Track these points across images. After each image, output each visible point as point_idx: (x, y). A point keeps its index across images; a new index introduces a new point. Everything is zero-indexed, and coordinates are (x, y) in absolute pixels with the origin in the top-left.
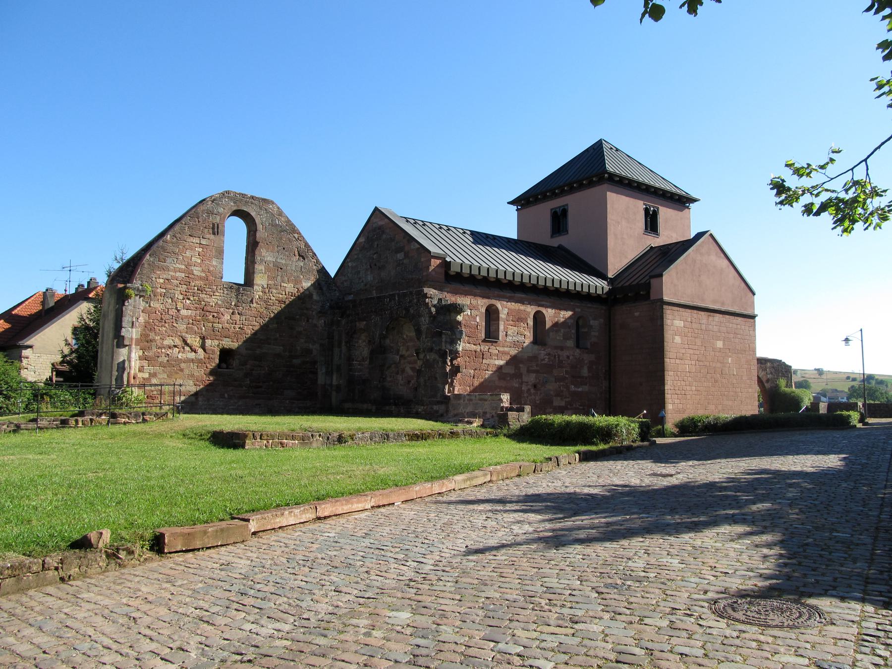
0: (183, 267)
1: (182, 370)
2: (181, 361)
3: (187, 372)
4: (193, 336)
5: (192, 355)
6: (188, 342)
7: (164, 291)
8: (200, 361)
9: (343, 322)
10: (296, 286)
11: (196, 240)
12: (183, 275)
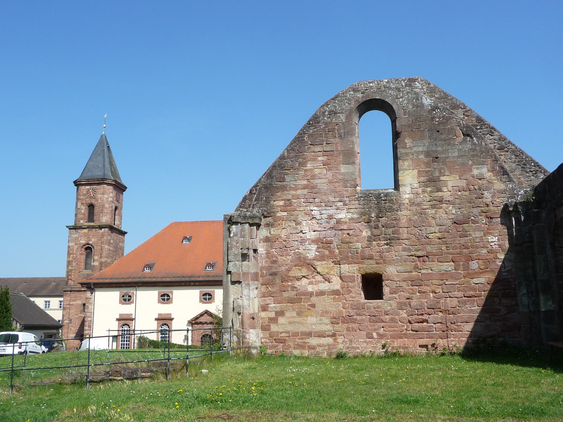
0: (305, 182)
1: (313, 306)
2: (311, 294)
3: (319, 308)
4: (324, 262)
5: (325, 286)
6: (319, 270)
7: (285, 214)
9: (544, 215)
10: (464, 177)
11: (318, 149)
12: (305, 191)
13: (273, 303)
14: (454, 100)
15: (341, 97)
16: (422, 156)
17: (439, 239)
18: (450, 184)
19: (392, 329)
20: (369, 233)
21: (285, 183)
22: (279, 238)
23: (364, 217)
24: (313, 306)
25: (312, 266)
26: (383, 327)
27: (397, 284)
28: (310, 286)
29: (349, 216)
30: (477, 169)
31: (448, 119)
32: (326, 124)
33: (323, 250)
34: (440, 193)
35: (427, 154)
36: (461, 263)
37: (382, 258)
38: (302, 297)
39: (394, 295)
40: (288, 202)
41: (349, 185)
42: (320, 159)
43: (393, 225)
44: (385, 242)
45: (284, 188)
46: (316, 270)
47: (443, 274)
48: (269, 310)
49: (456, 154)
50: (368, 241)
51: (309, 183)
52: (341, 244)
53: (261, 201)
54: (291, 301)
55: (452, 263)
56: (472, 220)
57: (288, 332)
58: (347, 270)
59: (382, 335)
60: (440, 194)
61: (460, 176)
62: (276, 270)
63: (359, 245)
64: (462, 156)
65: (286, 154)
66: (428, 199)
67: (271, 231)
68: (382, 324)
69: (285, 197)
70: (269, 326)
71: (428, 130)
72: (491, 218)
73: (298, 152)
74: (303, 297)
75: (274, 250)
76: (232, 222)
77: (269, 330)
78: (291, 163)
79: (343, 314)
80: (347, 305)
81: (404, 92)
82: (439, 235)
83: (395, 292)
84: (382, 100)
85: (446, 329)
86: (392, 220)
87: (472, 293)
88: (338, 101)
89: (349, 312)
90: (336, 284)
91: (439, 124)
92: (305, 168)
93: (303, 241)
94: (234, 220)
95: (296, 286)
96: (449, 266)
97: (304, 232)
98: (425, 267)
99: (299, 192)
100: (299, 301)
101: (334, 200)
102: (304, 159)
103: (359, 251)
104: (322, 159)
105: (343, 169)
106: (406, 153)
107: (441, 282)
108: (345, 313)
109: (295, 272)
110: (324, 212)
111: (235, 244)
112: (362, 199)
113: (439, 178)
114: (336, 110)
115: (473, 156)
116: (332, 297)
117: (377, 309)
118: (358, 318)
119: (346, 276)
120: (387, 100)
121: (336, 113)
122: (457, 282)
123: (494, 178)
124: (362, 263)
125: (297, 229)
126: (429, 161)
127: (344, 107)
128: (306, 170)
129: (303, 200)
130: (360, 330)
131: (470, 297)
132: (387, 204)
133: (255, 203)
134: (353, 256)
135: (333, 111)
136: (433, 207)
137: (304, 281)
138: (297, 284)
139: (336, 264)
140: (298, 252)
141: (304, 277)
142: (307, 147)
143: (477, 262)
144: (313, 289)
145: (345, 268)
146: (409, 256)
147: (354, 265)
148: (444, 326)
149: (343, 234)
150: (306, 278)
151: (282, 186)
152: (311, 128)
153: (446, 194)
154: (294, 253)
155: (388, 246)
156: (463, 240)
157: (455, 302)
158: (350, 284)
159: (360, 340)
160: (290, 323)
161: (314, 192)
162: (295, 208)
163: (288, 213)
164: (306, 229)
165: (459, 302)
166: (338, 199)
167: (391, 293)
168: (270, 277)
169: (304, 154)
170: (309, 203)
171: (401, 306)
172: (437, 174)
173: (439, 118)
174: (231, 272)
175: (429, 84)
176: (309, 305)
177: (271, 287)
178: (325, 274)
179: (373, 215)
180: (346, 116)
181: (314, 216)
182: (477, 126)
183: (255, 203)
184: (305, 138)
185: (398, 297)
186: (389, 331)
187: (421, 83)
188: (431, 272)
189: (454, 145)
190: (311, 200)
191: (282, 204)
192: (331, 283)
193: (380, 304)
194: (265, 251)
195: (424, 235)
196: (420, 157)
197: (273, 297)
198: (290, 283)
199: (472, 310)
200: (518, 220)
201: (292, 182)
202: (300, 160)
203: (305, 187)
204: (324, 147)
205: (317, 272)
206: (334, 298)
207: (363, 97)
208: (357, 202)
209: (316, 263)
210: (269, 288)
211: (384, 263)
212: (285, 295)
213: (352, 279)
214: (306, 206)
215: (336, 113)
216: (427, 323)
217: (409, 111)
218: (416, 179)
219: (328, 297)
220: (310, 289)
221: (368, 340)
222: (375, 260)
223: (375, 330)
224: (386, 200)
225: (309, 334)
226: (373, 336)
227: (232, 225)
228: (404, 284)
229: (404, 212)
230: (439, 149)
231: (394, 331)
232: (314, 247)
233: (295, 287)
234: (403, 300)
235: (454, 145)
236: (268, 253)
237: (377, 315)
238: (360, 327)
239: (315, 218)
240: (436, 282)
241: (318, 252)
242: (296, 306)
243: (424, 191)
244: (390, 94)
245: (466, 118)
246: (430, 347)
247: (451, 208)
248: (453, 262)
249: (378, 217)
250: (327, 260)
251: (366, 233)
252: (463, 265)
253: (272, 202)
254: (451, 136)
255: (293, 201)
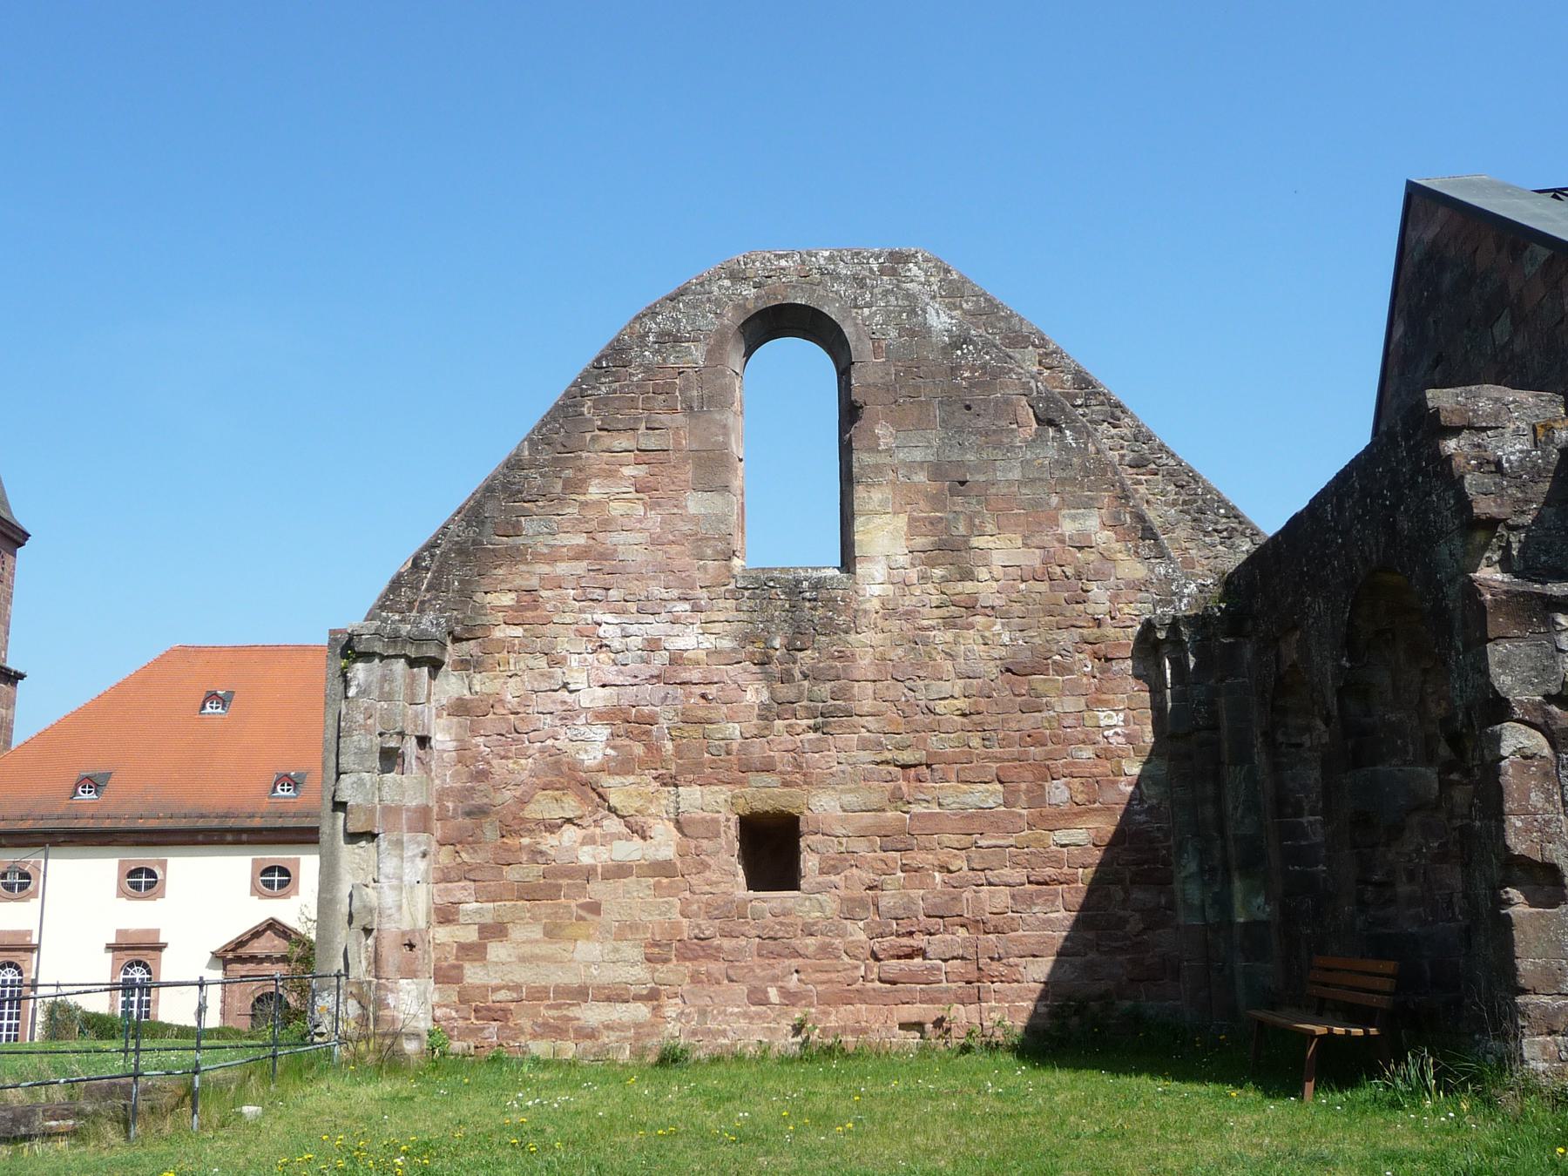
0: (581, 540)
1: (594, 908)
2: (589, 873)
4: (631, 779)
5: (629, 850)
6: (614, 800)
7: (519, 631)
8: (662, 869)
9: (1248, 652)
10: (1036, 541)
11: (622, 441)
12: (581, 567)
13: (473, 899)
14: (1015, 321)
15: (694, 293)
16: (921, 477)
17: (964, 715)
18: (998, 559)
19: (824, 977)
20: (765, 696)
21: (519, 540)
22: (496, 705)
23: (750, 648)
24: (594, 908)
25: (594, 790)
26: (797, 971)
27: (840, 843)
28: (585, 848)
29: (708, 642)
30: (1074, 518)
31: (996, 374)
32: (647, 368)
33: (627, 742)
34: (969, 583)
35: (937, 471)
36: (1023, 786)
37: (801, 767)
38: (561, 881)
39: (833, 878)
40: (528, 598)
41: (709, 552)
42: (626, 471)
43: (833, 672)
44: (811, 722)
45: (515, 556)
46: (605, 800)
47: (971, 816)
48: (461, 921)
49: (1016, 475)
50: (761, 717)
51: (591, 542)
52: (681, 724)
53: (447, 592)
54: (528, 893)
55: (999, 787)
56: (1055, 662)
57: (517, 988)
58: (698, 803)
59: (795, 994)
60: (969, 586)
61: (1025, 537)
62: (486, 800)
63: (734, 730)
64: (1033, 481)
65: (527, 453)
66: (936, 599)
67: (475, 681)
68: (795, 963)
69: (518, 582)
70: (460, 967)
71: (941, 402)
72: (1108, 660)
73: (563, 449)
74: (564, 882)
75: (481, 740)
76: (354, 652)
77: (458, 980)
78: (539, 481)
79: (681, 933)
80: (695, 907)
81: (876, 291)
82: (962, 704)
83: (834, 870)
84: (814, 309)
85: (976, 974)
86: (833, 658)
87: (1050, 871)
88: (686, 304)
89: (698, 926)
90: (664, 843)
91: (971, 385)
92: (582, 498)
93: (568, 715)
94: (361, 648)
95: (543, 848)
96: (988, 795)
97: (572, 687)
98: (922, 796)
99: (562, 568)
100: (552, 892)
101: (666, 596)
102: (580, 470)
103: (735, 746)
104: (634, 473)
105: (695, 504)
106: (877, 466)
107: (966, 841)
108: (687, 929)
109: (544, 807)
110: (632, 629)
111: (360, 718)
112: (747, 593)
113: (966, 542)
114: (678, 331)
115: (1062, 481)
116: (652, 881)
117: (781, 919)
118: (727, 943)
119: (692, 821)
120: (826, 310)
121: (677, 340)
122: (1011, 841)
123: (1118, 546)
124: (741, 783)
125: (550, 678)
126: (941, 491)
127: (701, 322)
128: (584, 504)
129: (572, 592)
130: (731, 981)
131: (1046, 883)
132: (820, 612)
133: (428, 596)
134: (715, 761)
135: (669, 334)
136: (949, 623)
137: (570, 834)
138: (548, 842)
139: (665, 784)
140: (553, 746)
141: (569, 821)
142: (588, 436)
143: (1067, 784)
144: (594, 857)
145: (693, 797)
146: (878, 764)
147: (716, 788)
148: (972, 967)
149: (689, 695)
150: (575, 824)
151: (511, 548)
152: (603, 380)
153: (985, 588)
154: (542, 751)
155: (819, 735)
156: (1029, 721)
157: (1002, 897)
158: (705, 843)
159: (730, 1010)
160: (523, 959)
161: (607, 569)
162: (547, 617)
163: (525, 630)
164: (578, 679)
165: (1013, 897)
166: (675, 593)
167: (822, 872)
168: (468, 821)
169: (581, 458)
170: (591, 603)
171: (851, 909)
172: (962, 530)
173: (973, 369)
174: (345, 803)
175: (947, 271)
176: (581, 906)
177: (468, 853)
178: (633, 812)
179: (777, 643)
180: (709, 352)
181: (605, 642)
182: (1076, 396)
183: (428, 596)
184: (585, 410)
185: (842, 884)
186: (815, 983)
187: (924, 266)
188: (938, 810)
189: (1011, 448)
190: (598, 594)
191: (511, 603)
192: (649, 841)
193: (789, 904)
194: (455, 744)
195: (922, 703)
196: (916, 478)
197: (474, 881)
198: (526, 841)
199: (1049, 920)
200: (1179, 667)
201: (541, 538)
202: (569, 473)
203: (580, 555)
204: (641, 439)
205: (609, 809)
206: (657, 886)
207: (757, 298)
208: (731, 603)
209: (607, 780)
210: (463, 855)
211: (806, 783)
212: (512, 874)
213: (711, 829)
214: (581, 611)
215: (677, 340)
216: (925, 958)
217: (888, 346)
218: (904, 543)
219: (639, 883)
220: (586, 857)
221: (753, 1008)
222: (781, 773)
223: (775, 979)
224: (815, 600)
225: (581, 994)
226: (768, 998)
227: (355, 661)
228: (860, 846)
229: (868, 637)
230: (971, 457)
231: (830, 981)
232: (601, 733)
233: (541, 852)
234: (859, 892)
235: (1011, 448)
236: (462, 748)
237: (781, 934)
238: (731, 972)
239: (607, 646)
240: (952, 839)
241: (613, 748)
242: (545, 907)
243: (924, 578)
244: (837, 292)
245: (1046, 373)
246: (929, 1027)
247: (998, 627)
248: (1001, 782)
249: (791, 648)
250: (638, 771)
251: (755, 694)
252: (1028, 791)
253: (479, 597)
254: (1003, 423)
255: (544, 593)
